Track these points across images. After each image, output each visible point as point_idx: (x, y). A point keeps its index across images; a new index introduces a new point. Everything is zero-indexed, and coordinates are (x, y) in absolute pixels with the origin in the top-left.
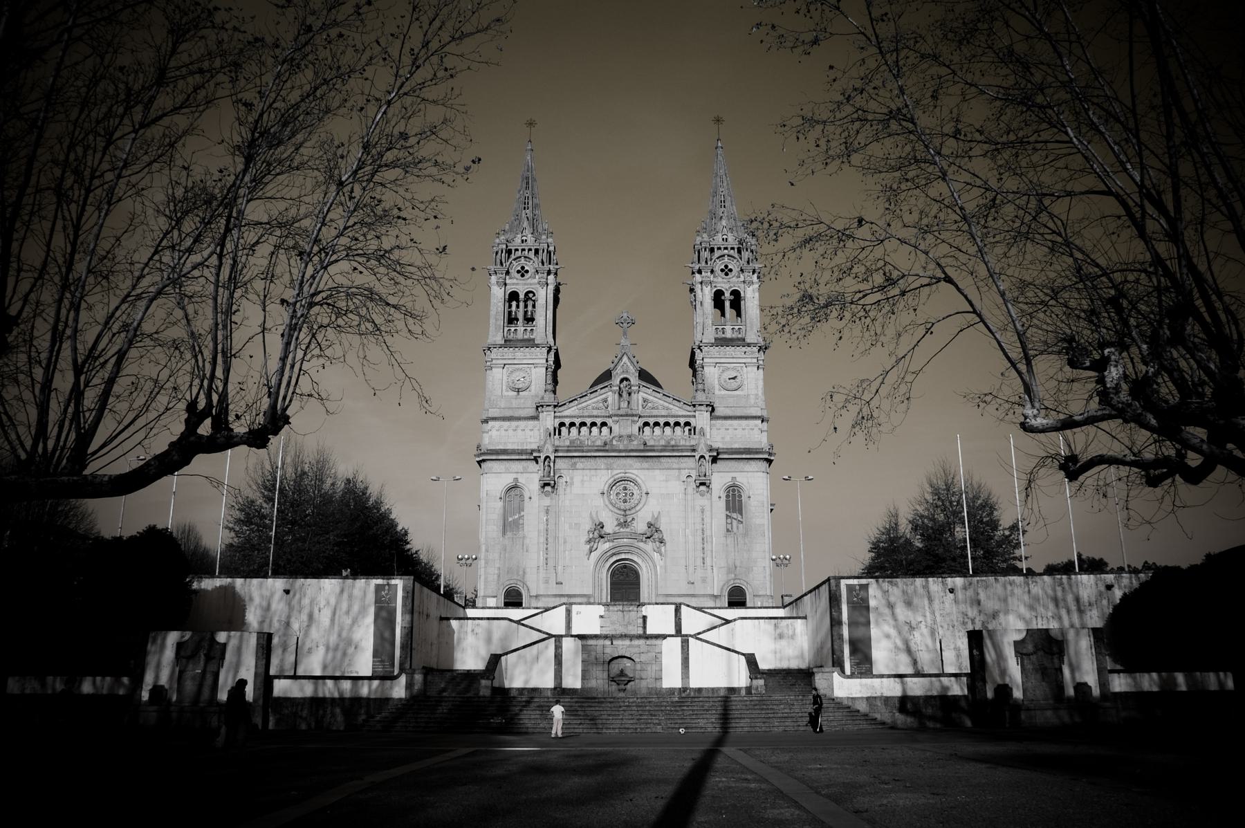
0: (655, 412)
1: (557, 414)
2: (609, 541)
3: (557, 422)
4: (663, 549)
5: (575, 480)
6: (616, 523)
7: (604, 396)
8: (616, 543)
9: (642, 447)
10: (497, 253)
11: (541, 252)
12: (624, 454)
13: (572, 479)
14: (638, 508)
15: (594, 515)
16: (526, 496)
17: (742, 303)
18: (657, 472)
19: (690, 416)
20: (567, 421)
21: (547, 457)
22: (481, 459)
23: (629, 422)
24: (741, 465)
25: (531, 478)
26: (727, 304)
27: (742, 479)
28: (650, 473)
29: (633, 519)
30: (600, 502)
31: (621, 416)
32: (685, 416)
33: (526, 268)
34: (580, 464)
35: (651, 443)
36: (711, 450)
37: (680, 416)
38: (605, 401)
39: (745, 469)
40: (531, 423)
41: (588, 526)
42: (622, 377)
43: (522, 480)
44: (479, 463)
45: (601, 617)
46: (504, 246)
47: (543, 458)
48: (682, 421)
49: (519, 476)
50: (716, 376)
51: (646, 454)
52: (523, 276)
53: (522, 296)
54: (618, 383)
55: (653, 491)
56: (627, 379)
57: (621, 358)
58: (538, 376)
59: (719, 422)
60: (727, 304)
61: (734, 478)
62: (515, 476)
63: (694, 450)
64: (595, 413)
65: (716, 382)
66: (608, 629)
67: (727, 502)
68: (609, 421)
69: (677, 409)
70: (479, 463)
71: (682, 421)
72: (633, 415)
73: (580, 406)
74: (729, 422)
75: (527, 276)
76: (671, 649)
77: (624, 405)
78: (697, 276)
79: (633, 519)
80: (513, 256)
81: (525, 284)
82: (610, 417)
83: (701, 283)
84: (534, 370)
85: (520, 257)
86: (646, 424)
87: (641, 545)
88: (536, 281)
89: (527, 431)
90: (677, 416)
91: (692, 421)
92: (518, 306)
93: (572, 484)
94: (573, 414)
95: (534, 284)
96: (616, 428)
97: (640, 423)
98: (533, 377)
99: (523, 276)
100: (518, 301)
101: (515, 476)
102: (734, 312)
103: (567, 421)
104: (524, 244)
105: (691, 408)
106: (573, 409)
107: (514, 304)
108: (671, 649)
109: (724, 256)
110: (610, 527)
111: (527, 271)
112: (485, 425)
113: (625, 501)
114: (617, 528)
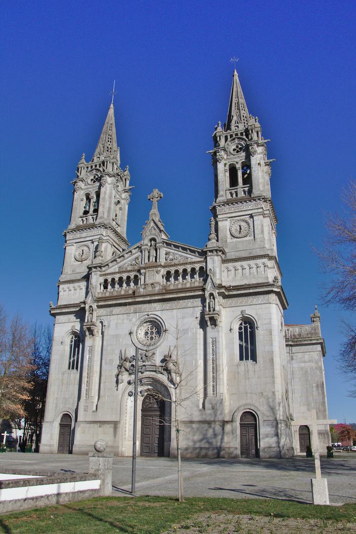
0: (176, 262)
3: (102, 280)
4: (177, 379)
12: (148, 299)
14: (158, 344)
24: (250, 299)
27: (250, 312)
29: (154, 354)
32: (199, 262)
39: (254, 303)
42: (150, 237)
50: (228, 228)
51: (166, 297)
59: (230, 265)
61: (242, 312)
62: (73, 324)
64: (129, 268)
65: (228, 233)
67: (240, 334)
69: (193, 257)
71: (197, 267)
72: (156, 267)
74: (238, 264)
86: (168, 273)
90: (191, 263)
93: (109, 326)
94: (113, 271)
97: (163, 271)
103: (109, 278)
109: (234, 139)
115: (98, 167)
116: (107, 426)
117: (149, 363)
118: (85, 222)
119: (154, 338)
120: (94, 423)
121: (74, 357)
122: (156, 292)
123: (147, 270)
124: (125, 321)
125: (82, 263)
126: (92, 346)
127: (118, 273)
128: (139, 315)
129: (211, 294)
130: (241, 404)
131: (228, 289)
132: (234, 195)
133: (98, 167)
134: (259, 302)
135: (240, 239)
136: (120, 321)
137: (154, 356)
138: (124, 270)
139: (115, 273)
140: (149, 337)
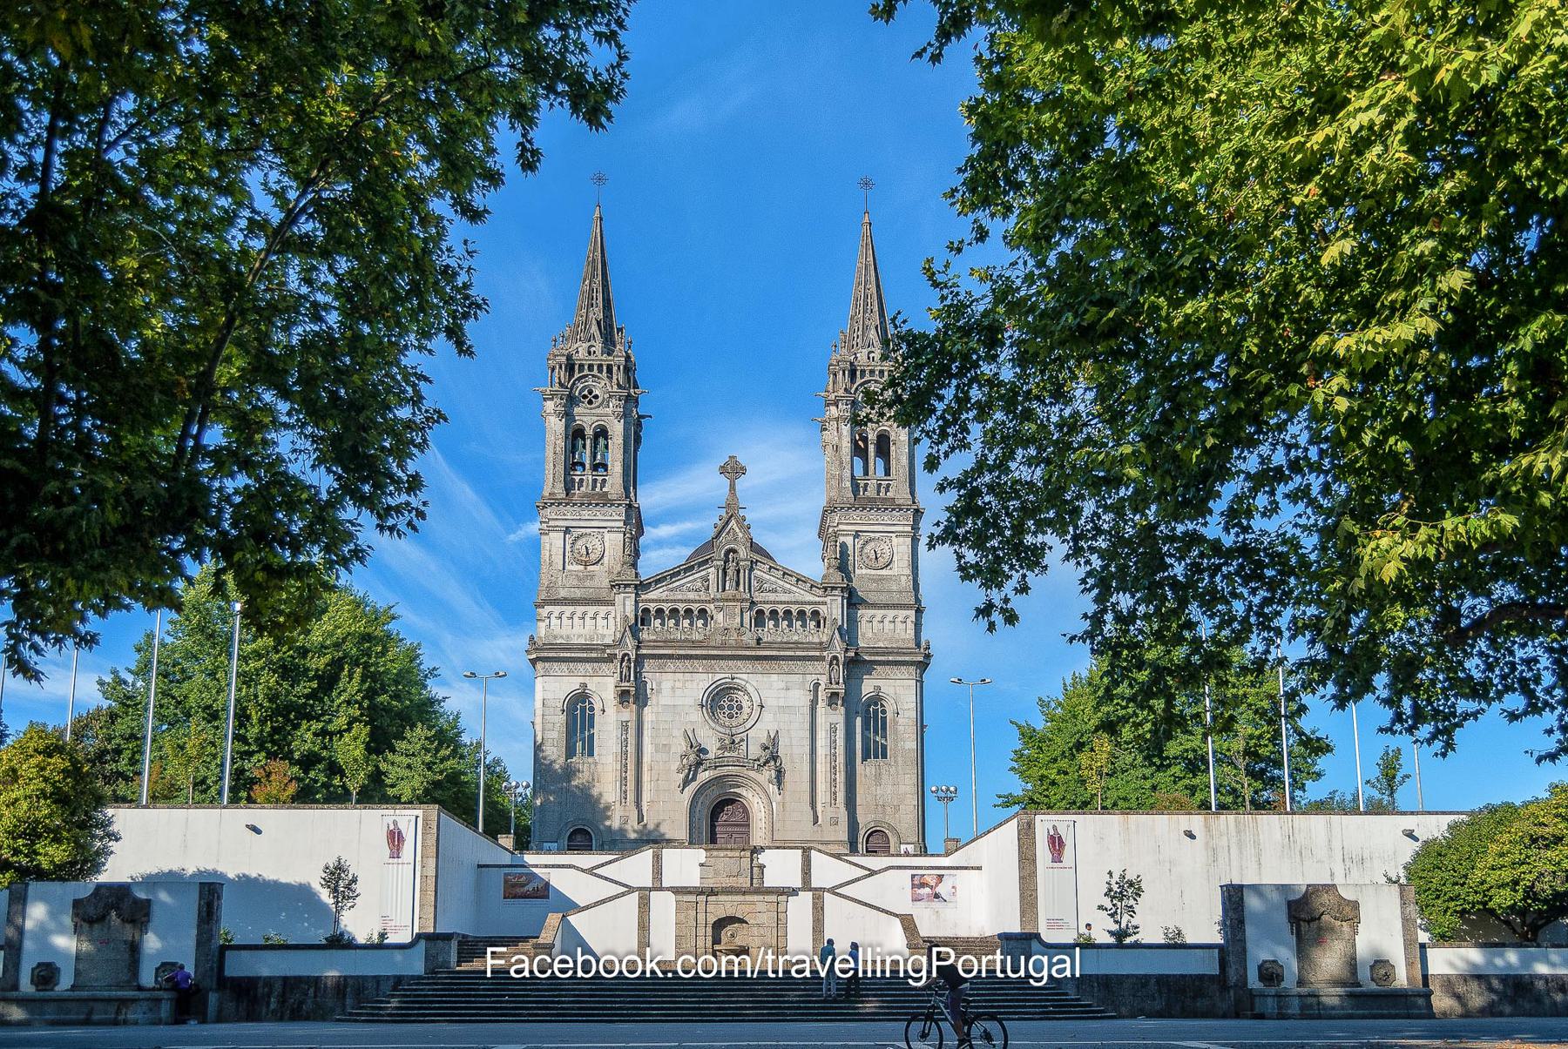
0: (772, 597)
5: (664, 686)
6: (718, 745)
7: (703, 573)
8: (718, 772)
10: (553, 370)
11: (615, 369)
13: (659, 684)
16: (597, 706)
17: (893, 448)
18: (775, 677)
19: (819, 603)
20: (652, 607)
22: (534, 656)
25: (604, 687)
26: (872, 448)
28: (765, 678)
30: (697, 717)
31: (727, 600)
33: (596, 392)
34: (671, 665)
37: (806, 603)
40: (603, 610)
41: (681, 746)
43: (592, 684)
44: (533, 662)
45: (702, 865)
46: (564, 359)
47: (619, 657)
48: (808, 609)
49: (587, 680)
51: (763, 657)
53: (589, 432)
55: (768, 703)
56: (735, 551)
57: (727, 523)
58: (613, 544)
60: (872, 448)
62: (581, 680)
63: (825, 649)
64: (691, 596)
66: (712, 881)
68: (710, 608)
70: (533, 662)
72: (743, 600)
75: (596, 403)
76: (799, 910)
78: (833, 409)
80: (577, 375)
81: (594, 415)
83: (837, 419)
84: (607, 536)
85: (586, 376)
87: (752, 774)
88: (609, 411)
90: (802, 603)
91: (823, 610)
92: (584, 446)
93: (659, 691)
95: (607, 415)
96: (719, 617)
99: (590, 402)
100: (584, 439)
101: (581, 680)
102: (880, 463)
103: (652, 607)
104: (592, 357)
105: (821, 592)
107: (581, 442)
108: (799, 910)
111: (596, 397)
112: (540, 610)
113: (731, 716)
115: (595, 372)
129: (835, 658)
130: (869, 819)
133: (595, 372)
134: (899, 676)
135: (873, 572)
136: (678, 685)
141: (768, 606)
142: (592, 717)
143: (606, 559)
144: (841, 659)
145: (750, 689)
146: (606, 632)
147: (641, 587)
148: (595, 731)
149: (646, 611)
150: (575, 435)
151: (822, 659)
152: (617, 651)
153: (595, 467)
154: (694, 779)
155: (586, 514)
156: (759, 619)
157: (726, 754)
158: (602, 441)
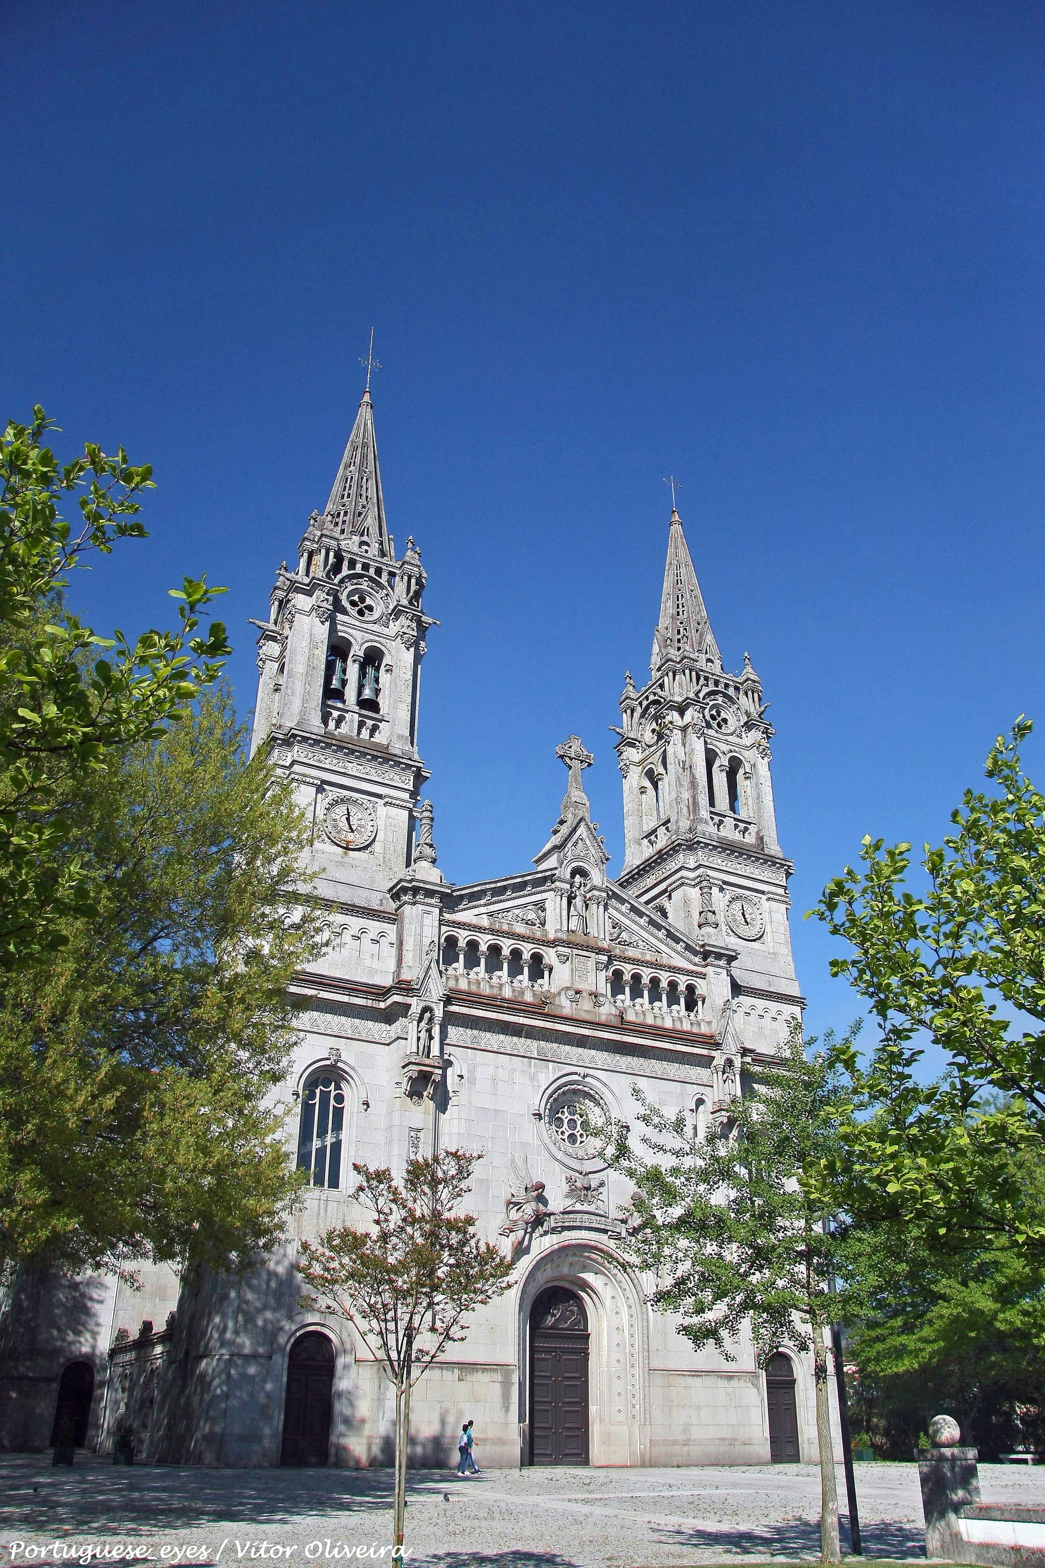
0: (631, 953)
1: (447, 916)
2: (554, 1230)
5: (479, 1072)
6: (566, 1188)
9: (616, 1022)
13: (472, 1070)
15: (519, 1162)
21: (426, 1009)
23: (591, 964)
29: (602, 1184)
33: (369, 601)
35: (630, 1016)
36: (745, 1052)
38: (541, 906)
40: (375, 927)
52: (361, 613)
54: (568, 876)
62: (333, 1042)
63: (717, 1046)
64: (520, 929)
69: (673, 954)
71: (683, 981)
73: (492, 908)
77: (574, 924)
79: (602, 1184)
80: (345, 571)
81: (366, 631)
82: (553, 943)
89: (366, 939)
93: (473, 1081)
94: (475, 921)
95: (387, 637)
98: (381, 823)
103: (463, 937)
106: (476, 911)
110: (557, 1200)
111: (370, 608)
114: (569, 1202)
116: (482, 1378)
117: (591, 1208)
118: (365, 734)
119: (579, 1139)
120: (442, 1368)
121: (321, 1151)
122: (603, 1019)
123: (576, 951)
124: (517, 1076)
125: (346, 854)
126: (419, 1130)
127: (492, 931)
128: (554, 1069)
131: (759, 1059)
132: (332, 724)
137: (601, 1190)
138: (505, 927)
139: (480, 929)
140: (567, 1134)
141: (629, 967)
142: (339, 1113)
143: (377, 847)
144: (737, 1062)
145: (608, 1097)
146: (376, 965)
147: (449, 901)
148: (344, 1136)
149: (451, 941)
150: (338, 649)
151: (706, 1062)
152: (413, 1001)
153: (363, 704)
154: (527, 1250)
155: (353, 768)
156: (617, 982)
157: (578, 1207)
158: (370, 671)
